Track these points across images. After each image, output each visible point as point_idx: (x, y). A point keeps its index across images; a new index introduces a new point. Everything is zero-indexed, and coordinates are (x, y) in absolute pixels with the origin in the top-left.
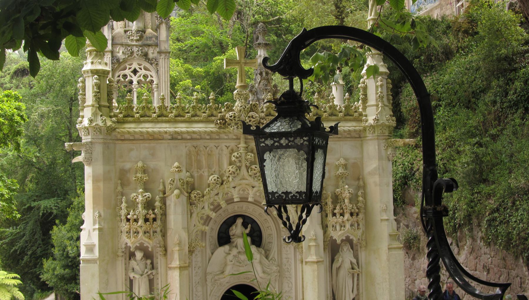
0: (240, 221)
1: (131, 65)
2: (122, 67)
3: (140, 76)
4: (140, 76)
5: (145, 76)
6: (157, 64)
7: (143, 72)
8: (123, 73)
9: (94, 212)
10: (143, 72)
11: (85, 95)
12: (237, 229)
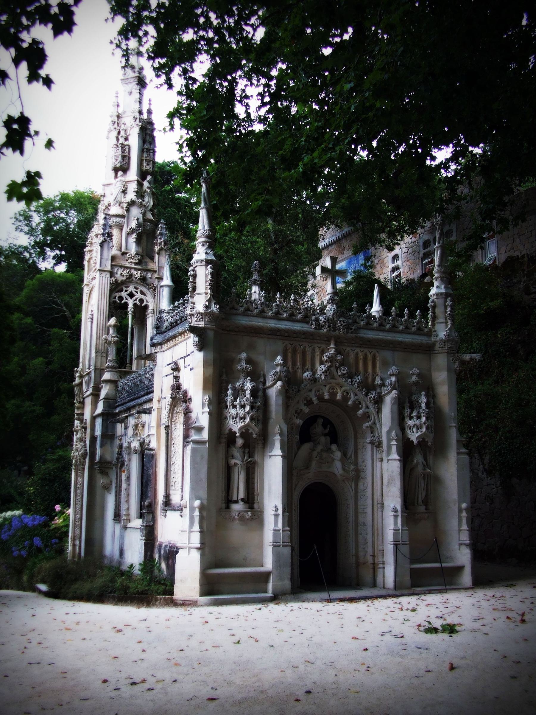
0: (320, 421)
1: (128, 287)
2: (119, 288)
3: (135, 300)
4: (135, 300)
5: (141, 301)
6: (155, 289)
7: (139, 296)
8: (119, 294)
9: (204, 395)
10: (139, 296)
11: (195, 283)
12: (318, 428)
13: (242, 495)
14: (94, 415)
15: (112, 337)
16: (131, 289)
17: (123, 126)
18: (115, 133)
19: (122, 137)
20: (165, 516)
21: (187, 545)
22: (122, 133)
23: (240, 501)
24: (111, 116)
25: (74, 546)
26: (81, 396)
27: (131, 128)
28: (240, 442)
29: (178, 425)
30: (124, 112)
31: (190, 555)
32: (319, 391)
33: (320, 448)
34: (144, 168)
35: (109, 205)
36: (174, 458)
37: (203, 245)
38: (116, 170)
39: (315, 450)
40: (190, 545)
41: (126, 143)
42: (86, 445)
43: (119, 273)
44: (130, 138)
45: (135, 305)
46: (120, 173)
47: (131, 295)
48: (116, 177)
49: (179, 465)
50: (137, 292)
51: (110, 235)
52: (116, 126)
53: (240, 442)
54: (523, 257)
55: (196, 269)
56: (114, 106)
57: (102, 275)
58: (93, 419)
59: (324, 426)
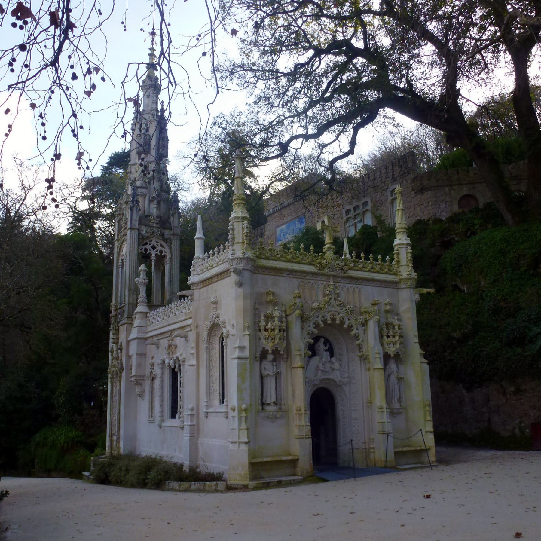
1: (151, 241)
3: (157, 251)
4: (157, 251)
5: (161, 252)
6: (171, 243)
7: (159, 248)
8: (145, 247)
10: (159, 248)
12: (321, 346)
13: (273, 399)
14: (129, 339)
16: (154, 243)
17: (144, 121)
20: (207, 417)
21: (237, 440)
22: (144, 126)
23: (272, 404)
25: (112, 441)
28: (270, 357)
29: (214, 346)
32: (323, 317)
33: (324, 359)
35: (135, 179)
37: (238, 206)
40: (240, 440)
41: (147, 133)
42: (122, 363)
43: (144, 231)
45: (156, 255)
47: (154, 248)
51: (137, 202)
53: (270, 357)
54: (429, 220)
55: (235, 223)
58: (128, 342)
59: (325, 344)
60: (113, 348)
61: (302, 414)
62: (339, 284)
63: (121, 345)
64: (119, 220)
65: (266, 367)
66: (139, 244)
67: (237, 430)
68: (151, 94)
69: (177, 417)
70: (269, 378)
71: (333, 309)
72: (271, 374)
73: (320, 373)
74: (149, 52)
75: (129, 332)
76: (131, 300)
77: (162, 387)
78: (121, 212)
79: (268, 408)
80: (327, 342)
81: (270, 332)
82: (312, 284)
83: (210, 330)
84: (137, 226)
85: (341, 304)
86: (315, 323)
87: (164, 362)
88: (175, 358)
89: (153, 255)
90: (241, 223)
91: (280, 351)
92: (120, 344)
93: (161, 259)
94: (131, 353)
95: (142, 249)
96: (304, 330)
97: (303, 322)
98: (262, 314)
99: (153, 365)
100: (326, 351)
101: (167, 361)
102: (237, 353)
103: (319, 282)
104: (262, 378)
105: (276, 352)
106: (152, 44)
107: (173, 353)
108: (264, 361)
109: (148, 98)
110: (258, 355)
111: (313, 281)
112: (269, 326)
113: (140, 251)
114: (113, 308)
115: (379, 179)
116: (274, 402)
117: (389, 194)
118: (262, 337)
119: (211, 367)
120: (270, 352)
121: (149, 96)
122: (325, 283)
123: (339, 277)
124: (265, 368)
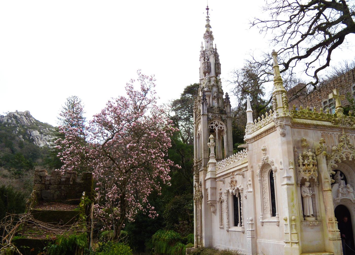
3: (219, 127)
4: (219, 127)
6: (227, 122)
7: (220, 125)
10: (220, 125)
11: (276, 103)
13: (312, 213)
14: (205, 179)
15: (212, 143)
16: (216, 122)
17: (206, 55)
18: (203, 58)
19: (206, 59)
20: (263, 225)
21: (290, 241)
22: (206, 58)
23: (311, 216)
24: (201, 52)
25: (197, 239)
26: (197, 171)
27: (210, 55)
28: (307, 184)
29: (265, 179)
30: (206, 50)
31: (292, 247)
32: (340, 156)
33: (342, 186)
34: (217, 72)
35: (203, 87)
36: (265, 195)
37: (278, 84)
38: (205, 73)
39: (340, 187)
43: (211, 116)
44: (210, 59)
45: (218, 129)
46: (207, 74)
47: (217, 125)
48: (205, 76)
49: (267, 199)
50: (219, 124)
51: (206, 100)
52: (203, 55)
53: (307, 184)
55: (276, 96)
56: (201, 47)
57: (204, 117)
58: (205, 181)
59: (341, 175)
60: (196, 185)
61: (333, 223)
62: (349, 134)
63: (201, 183)
64: (195, 112)
65: (305, 190)
66: (208, 123)
67: (290, 234)
68: (209, 41)
69: (239, 225)
70: (307, 198)
71: (346, 151)
72: (309, 195)
73: (340, 194)
74: (206, 19)
75: (205, 175)
76: (205, 156)
77: (228, 207)
78: (197, 107)
79: (308, 219)
80: (342, 174)
81: (306, 166)
82: (331, 134)
83: (261, 168)
84: (207, 113)
85: (351, 147)
86: (335, 161)
87: (228, 191)
88: (236, 188)
89: (217, 130)
90: (280, 95)
91: (314, 179)
92: (200, 182)
93: (221, 131)
94: (207, 187)
95: (210, 127)
96: (329, 165)
97: (327, 160)
98: (300, 155)
99: (221, 194)
100: (342, 179)
101: (230, 191)
102: (286, 181)
103: (335, 133)
104: (302, 198)
105: (311, 180)
106: (208, 14)
107: (234, 185)
108: (303, 186)
109: (208, 43)
110: (299, 183)
111: (331, 133)
112: (306, 162)
113: (209, 128)
114: (195, 161)
115: (344, 81)
116: (312, 215)
117: (352, 89)
118: (301, 170)
119: (264, 193)
120: (308, 180)
121: (208, 41)
122: (339, 133)
123: (348, 129)
124: (304, 191)
